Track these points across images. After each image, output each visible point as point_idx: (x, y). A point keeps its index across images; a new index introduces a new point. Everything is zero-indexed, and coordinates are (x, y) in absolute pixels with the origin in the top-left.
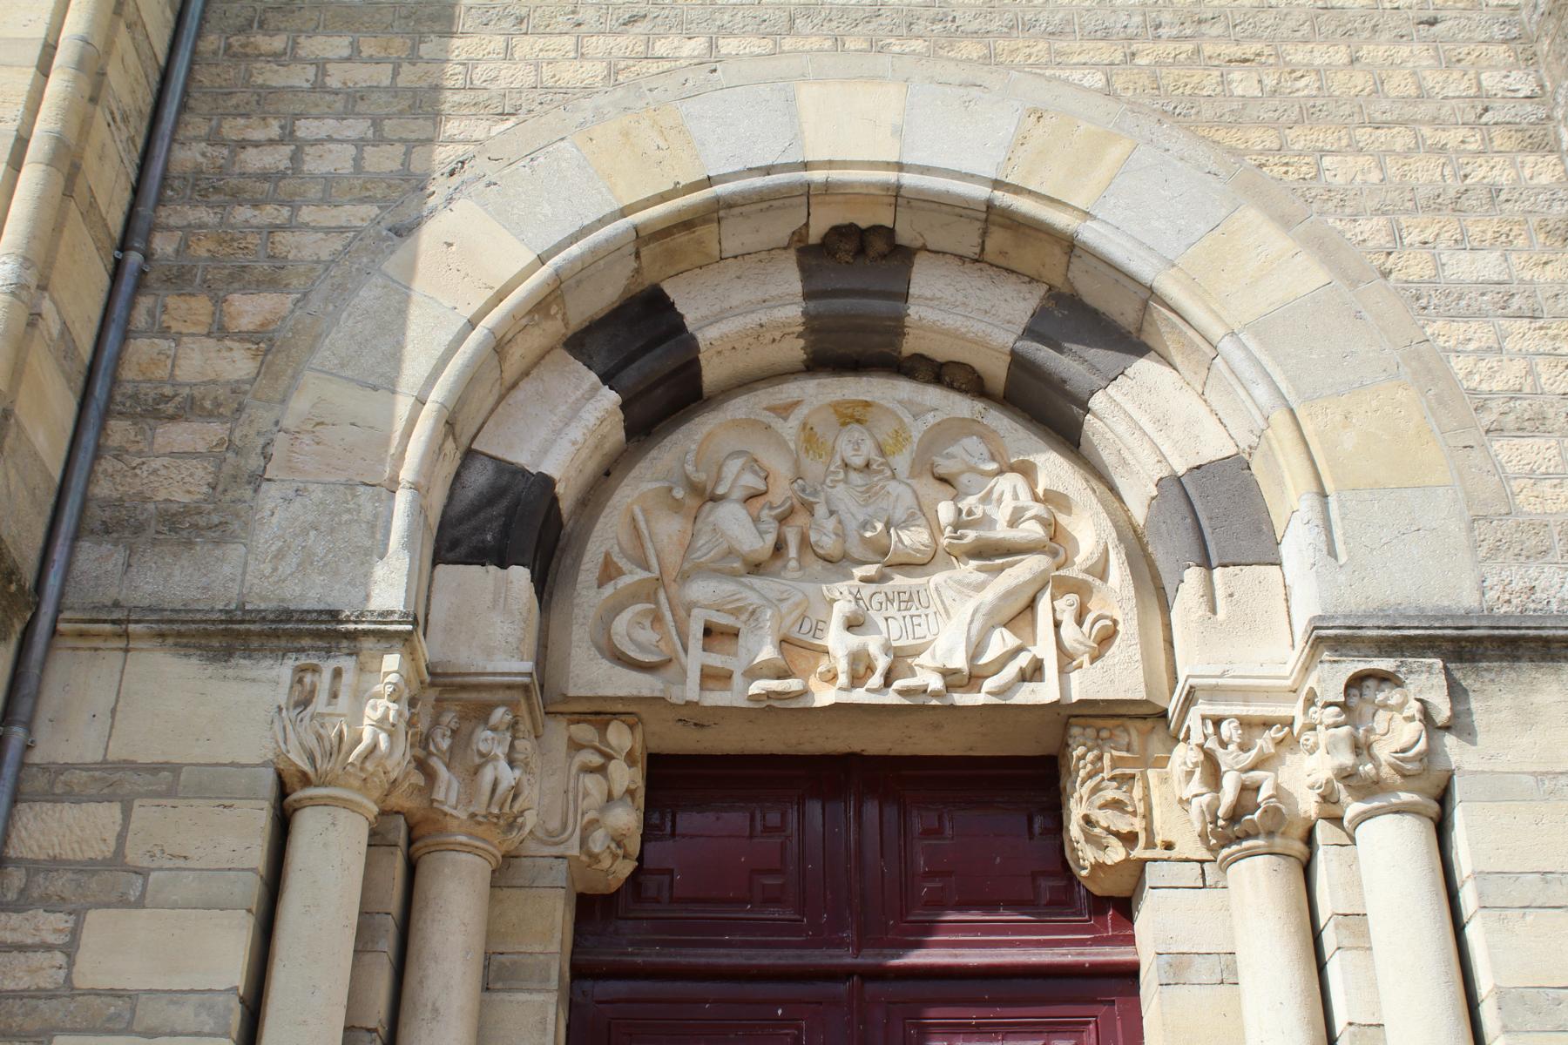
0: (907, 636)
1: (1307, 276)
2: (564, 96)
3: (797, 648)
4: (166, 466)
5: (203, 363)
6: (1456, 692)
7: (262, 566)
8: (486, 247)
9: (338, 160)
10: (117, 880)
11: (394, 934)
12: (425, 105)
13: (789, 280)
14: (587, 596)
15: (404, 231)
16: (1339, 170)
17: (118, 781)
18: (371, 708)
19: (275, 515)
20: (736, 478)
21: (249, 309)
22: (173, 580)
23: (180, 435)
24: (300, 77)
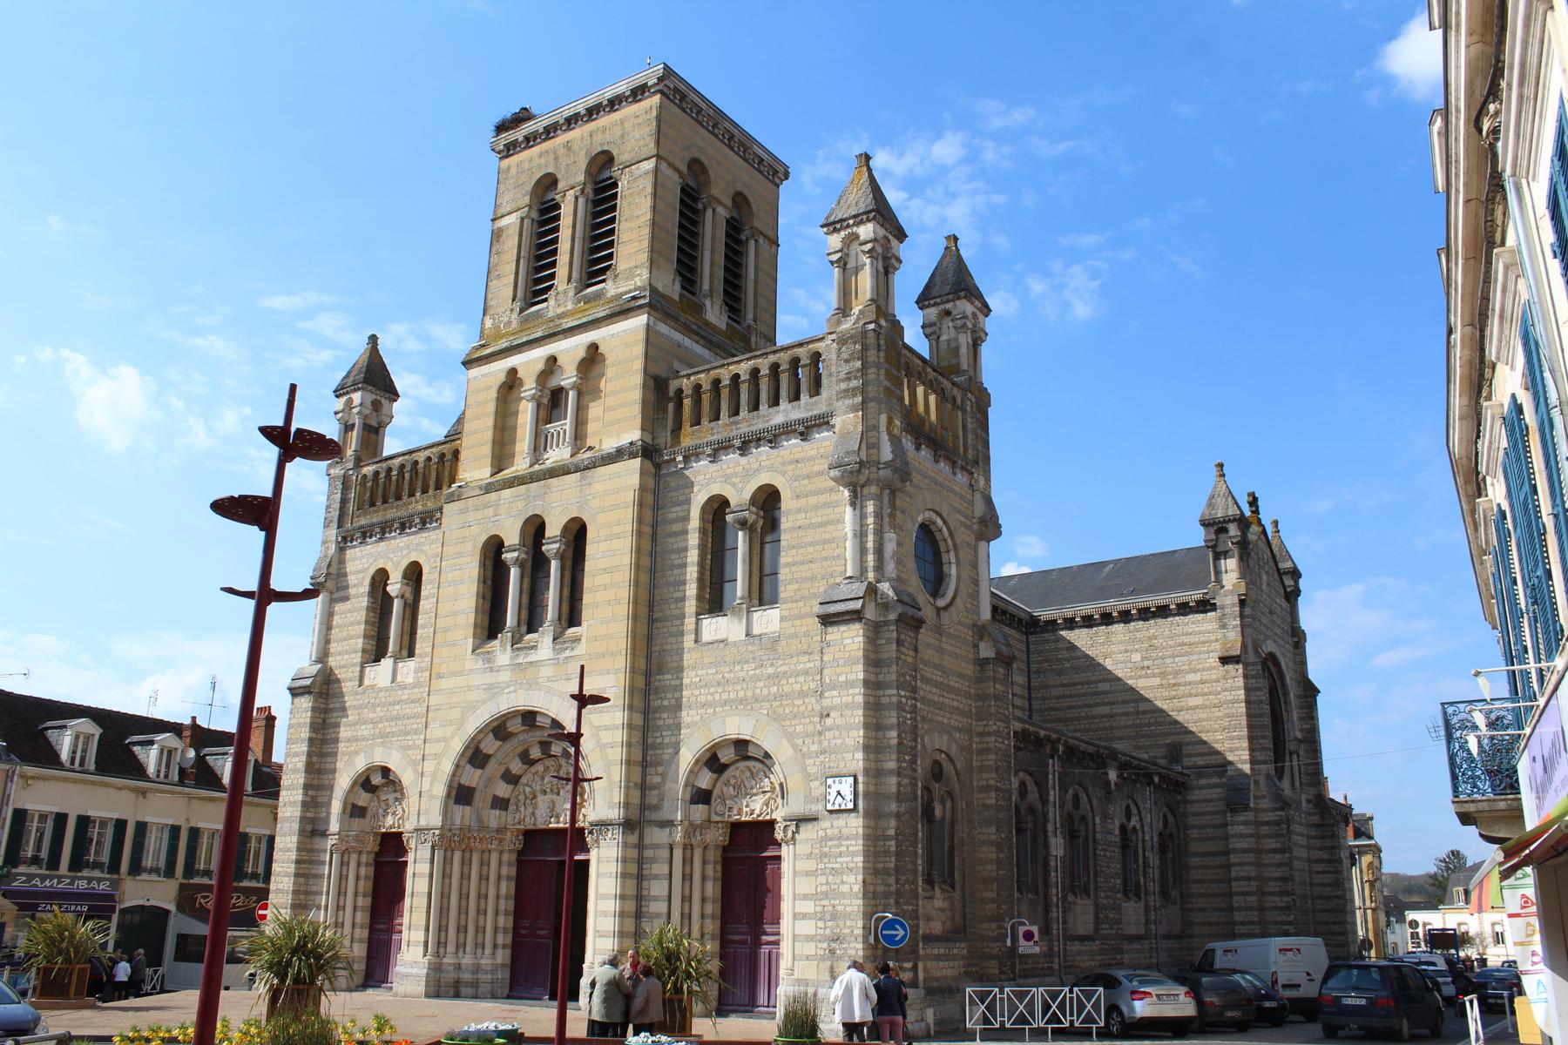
0: (754, 808)
1: (790, 752)
2: (695, 724)
3: (740, 812)
4: (652, 798)
5: (657, 779)
6: (797, 826)
7: (664, 815)
8: (687, 756)
9: (667, 740)
10: (653, 860)
11: (687, 861)
12: (678, 727)
13: (732, 749)
14: (713, 804)
15: (677, 753)
16: (799, 729)
17: (655, 846)
18: (678, 836)
19: (666, 805)
20: (733, 781)
21: (660, 769)
22: (655, 816)
23: (655, 792)
24: (661, 723)
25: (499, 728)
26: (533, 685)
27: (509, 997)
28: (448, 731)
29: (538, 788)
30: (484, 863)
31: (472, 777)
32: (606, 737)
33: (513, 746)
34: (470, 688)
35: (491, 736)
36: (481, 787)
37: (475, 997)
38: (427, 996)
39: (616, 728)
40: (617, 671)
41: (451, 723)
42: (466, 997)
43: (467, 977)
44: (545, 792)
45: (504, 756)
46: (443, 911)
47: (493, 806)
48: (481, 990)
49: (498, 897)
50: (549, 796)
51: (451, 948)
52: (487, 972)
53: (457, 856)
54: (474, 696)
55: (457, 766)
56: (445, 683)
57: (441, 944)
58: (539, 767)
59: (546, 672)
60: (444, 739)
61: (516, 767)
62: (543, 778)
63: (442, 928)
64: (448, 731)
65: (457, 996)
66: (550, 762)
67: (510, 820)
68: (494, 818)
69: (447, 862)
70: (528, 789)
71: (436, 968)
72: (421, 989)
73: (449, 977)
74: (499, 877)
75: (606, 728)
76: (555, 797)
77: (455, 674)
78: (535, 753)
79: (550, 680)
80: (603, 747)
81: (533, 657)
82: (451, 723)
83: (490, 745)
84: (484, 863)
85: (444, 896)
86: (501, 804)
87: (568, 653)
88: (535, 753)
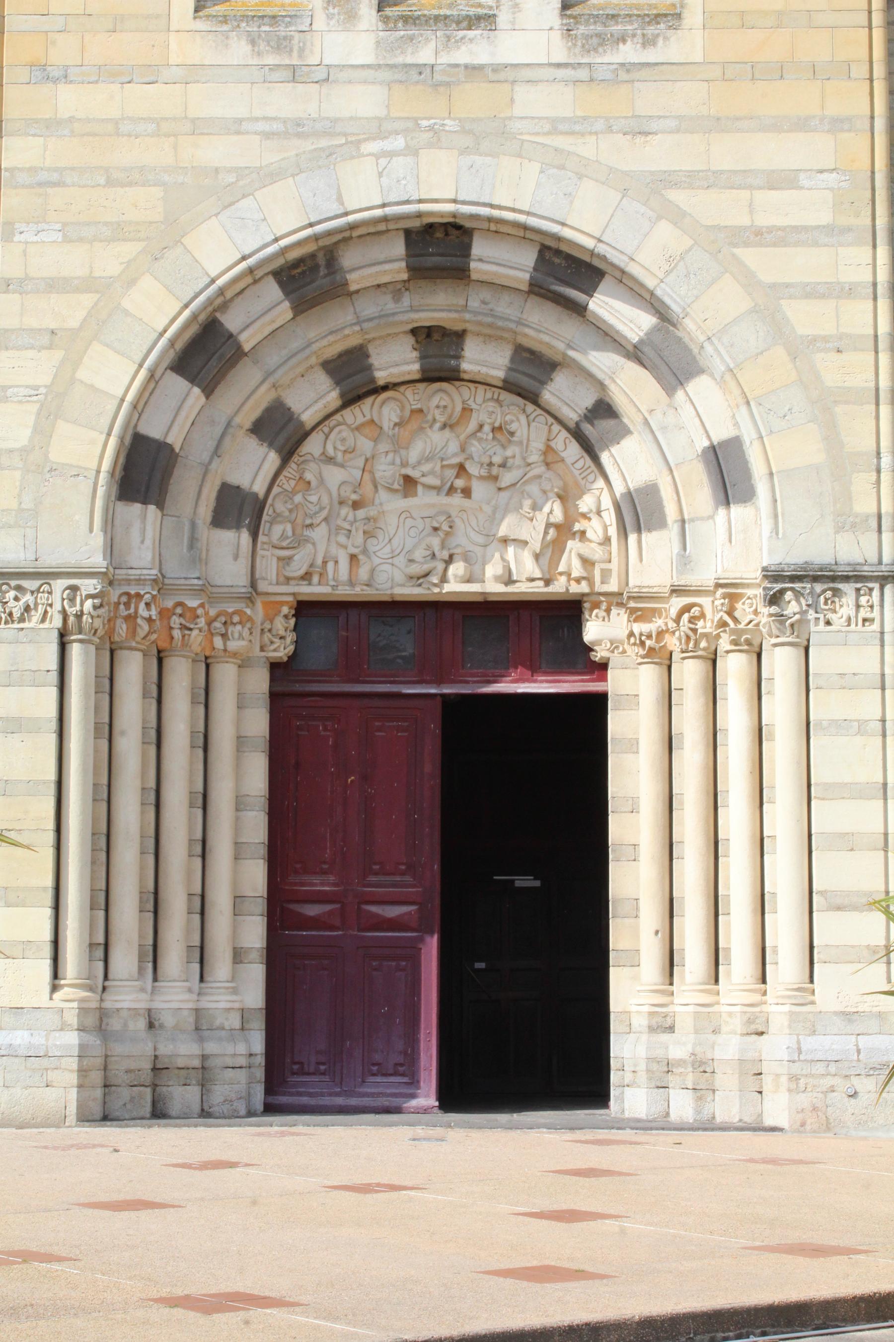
25: (308, 275)
26: (490, 136)
27: (270, 1109)
28: (110, 261)
29: (385, 470)
30: (205, 697)
31: (180, 413)
32: (806, 318)
33: (332, 330)
34: (199, 127)
35: (272, 291)
36: (200, 451)
37: (205, 1114)
38: (84, 1118)
39: (849, 292)
40: (837, 125)
41: (119, 232)
42: (184, 1117)
43: (184, 1050)
44: (409, 483)
45: (289, 366)
46: (104, 840)
47: (219, 520)
48: (219, 1093)
49: (240, 804)
50: (423, 499)
51: (125, 960)
52: (231, 1036)
53: (133, 670)
54: (216, 152)
55: (152, 376)
56: (69, 100)
57: (103, 949)
58: (386, 411)
59: (534, 102)
60: (88, 284)
61: (312, 398)
62: (398, 446)
63: (103, 900)
64: (110, 261)
65: (159, 1113)
66: (440, 399)
67: (268, 567)
68: (228, 556)
69: (108, 685)
70: (334, 476)
71: (98, 1023)
72: (63, 1091)
73: (135, 1052)
74: (241, 742)
75: (812, 292)
76: (457, 500)
77: (123, 75)
78: (395, 360)
79: (555, 126)
80: (800, 349)
81: (475, 49)
82: (119, 232)
83: (260, 317)
84: (205, 697)
85: (105, 795)
86: (238, 509)
87: (629, 52)
88: (395, 360)
